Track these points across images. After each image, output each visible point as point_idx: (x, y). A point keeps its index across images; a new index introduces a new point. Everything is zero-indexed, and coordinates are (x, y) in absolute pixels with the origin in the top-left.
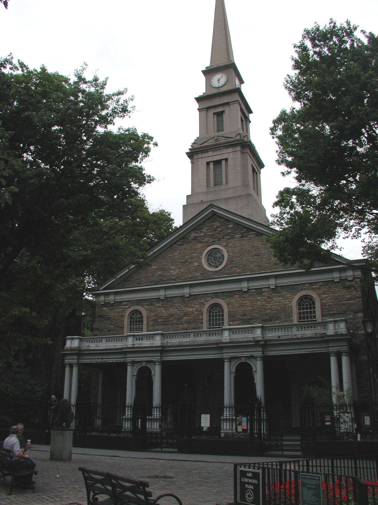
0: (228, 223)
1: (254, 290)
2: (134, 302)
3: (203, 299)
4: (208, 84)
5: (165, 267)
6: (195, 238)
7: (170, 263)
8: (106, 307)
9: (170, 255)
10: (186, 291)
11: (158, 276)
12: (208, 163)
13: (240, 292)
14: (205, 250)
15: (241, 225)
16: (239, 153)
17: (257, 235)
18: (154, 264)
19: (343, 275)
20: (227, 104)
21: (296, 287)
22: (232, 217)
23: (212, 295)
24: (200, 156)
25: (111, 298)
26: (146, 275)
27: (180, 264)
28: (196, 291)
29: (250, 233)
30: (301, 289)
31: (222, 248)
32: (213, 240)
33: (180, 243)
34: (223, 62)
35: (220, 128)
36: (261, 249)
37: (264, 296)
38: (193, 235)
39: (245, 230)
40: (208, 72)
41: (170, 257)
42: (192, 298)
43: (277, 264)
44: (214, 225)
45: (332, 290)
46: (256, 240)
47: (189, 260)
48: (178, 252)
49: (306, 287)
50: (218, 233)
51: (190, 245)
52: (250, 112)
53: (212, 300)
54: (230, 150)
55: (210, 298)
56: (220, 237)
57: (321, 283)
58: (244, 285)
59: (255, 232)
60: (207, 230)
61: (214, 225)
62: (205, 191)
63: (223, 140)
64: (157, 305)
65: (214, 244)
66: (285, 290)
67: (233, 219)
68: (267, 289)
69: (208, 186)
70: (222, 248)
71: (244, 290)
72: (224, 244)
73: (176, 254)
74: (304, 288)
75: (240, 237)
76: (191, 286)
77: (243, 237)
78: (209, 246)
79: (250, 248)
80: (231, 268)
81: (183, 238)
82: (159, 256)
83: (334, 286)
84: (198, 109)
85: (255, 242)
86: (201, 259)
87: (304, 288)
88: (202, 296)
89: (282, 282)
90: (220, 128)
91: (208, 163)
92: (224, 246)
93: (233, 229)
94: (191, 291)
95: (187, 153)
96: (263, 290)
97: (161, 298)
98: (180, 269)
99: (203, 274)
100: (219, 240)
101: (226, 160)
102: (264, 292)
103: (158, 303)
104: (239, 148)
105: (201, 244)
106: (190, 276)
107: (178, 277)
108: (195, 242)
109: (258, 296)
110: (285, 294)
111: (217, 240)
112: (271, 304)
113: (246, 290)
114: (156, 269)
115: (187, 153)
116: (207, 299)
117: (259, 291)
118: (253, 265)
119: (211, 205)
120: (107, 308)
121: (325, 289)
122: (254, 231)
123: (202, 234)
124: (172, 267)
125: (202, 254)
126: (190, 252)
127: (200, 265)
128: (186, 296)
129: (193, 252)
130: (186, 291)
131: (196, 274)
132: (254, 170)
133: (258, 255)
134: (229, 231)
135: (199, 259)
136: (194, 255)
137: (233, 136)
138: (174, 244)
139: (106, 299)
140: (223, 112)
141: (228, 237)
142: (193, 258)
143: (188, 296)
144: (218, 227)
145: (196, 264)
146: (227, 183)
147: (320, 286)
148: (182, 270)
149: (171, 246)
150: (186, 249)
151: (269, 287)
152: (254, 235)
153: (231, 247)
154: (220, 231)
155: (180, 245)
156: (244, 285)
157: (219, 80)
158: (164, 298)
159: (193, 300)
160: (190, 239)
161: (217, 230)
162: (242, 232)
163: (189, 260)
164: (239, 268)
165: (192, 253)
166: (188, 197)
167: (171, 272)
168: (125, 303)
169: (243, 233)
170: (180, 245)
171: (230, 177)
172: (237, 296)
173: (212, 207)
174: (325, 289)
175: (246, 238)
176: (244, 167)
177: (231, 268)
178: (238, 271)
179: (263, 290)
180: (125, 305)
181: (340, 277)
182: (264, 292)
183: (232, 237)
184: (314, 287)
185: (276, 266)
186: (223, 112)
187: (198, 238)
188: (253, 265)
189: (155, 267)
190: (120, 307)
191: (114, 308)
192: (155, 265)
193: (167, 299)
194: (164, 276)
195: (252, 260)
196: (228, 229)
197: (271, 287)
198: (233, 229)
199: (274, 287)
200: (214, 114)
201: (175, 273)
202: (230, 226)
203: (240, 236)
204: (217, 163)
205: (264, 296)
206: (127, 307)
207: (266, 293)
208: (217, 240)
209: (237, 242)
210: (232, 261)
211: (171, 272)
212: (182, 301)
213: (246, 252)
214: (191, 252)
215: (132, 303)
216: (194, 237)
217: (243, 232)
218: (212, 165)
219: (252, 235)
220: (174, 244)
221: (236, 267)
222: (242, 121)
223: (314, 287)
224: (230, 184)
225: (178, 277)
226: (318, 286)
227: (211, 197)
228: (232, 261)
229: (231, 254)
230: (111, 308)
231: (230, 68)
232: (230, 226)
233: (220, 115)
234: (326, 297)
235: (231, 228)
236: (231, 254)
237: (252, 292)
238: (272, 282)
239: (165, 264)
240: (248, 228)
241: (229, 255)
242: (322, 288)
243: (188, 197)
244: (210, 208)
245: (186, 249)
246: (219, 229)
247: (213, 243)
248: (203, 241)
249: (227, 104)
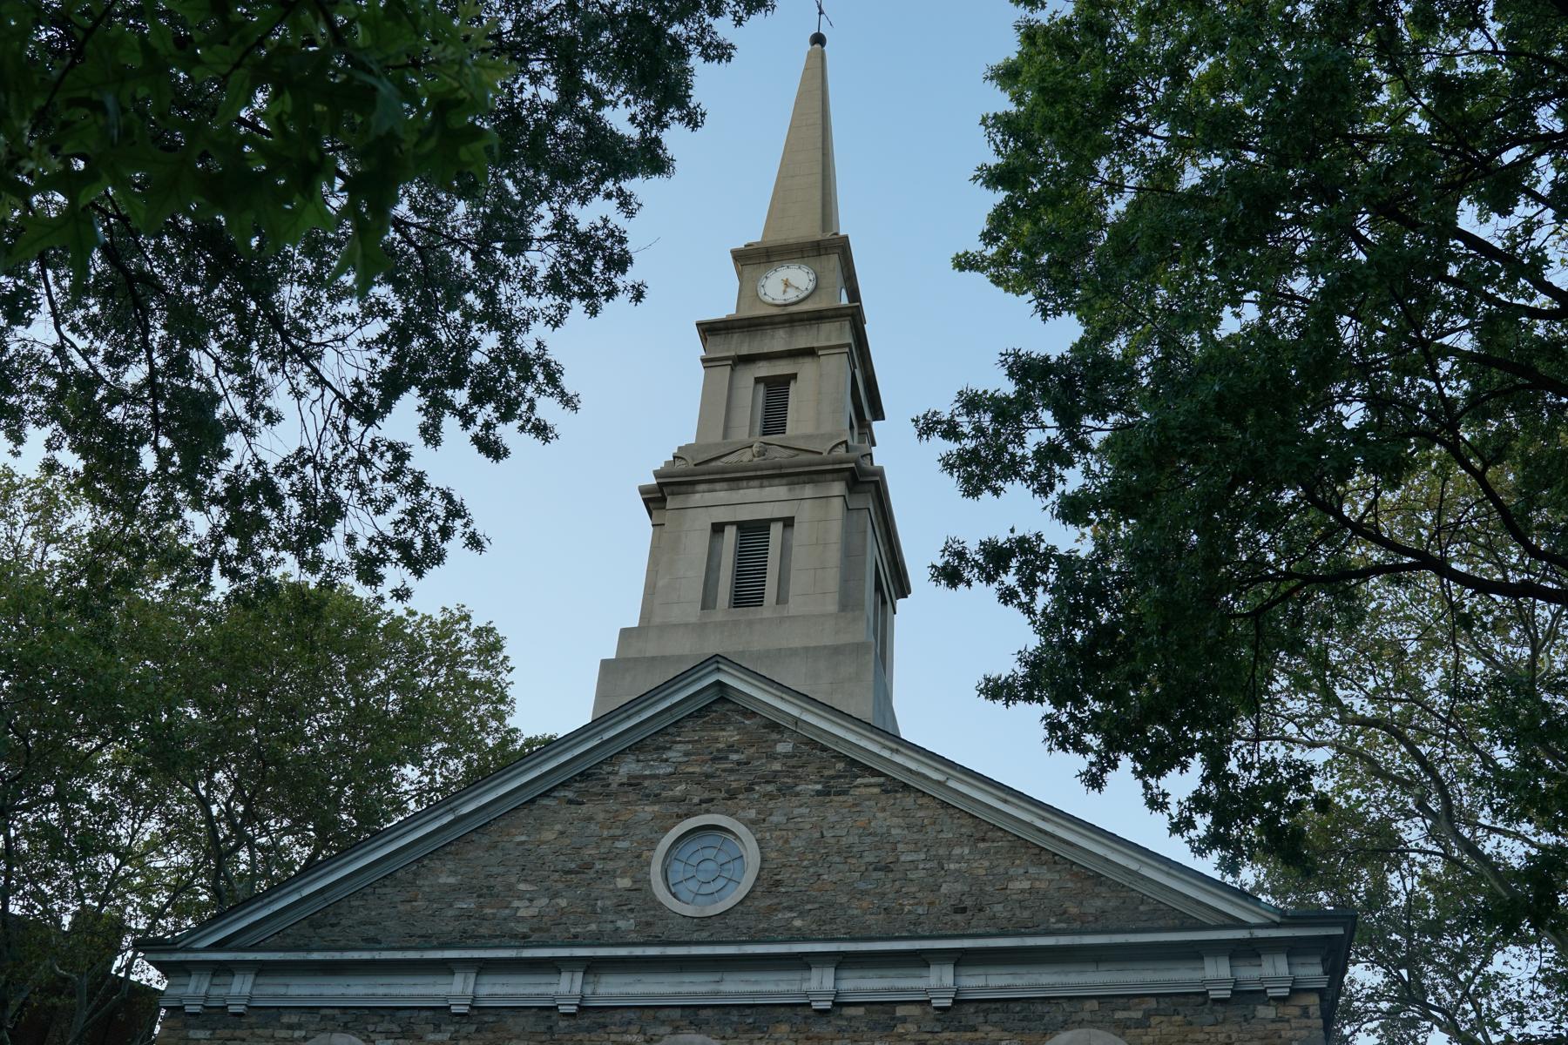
0: (775, 736)
1: (861, 1011)
2: (333, 1018)
3: (634, 1029)
4: (748, 291)
5: (492, 881)
6: (634, 783)
7: (514, 870)
8: (204, 1027)
9: (523, 838)
10: (567, 987)
11: (457, 918)
12: (718, 528)
13: (799, 1010)
14: (667, 830)
15: (824, 749)
16: (837, 504)
17: (886, 792)
18: (450, 865)
19: (1249, 973)
20: (810, 352)
21: (1039, 1008)
22: (795, 712)
23: (679, 1012)
24: (697, 499)
25: (241, 986)
26: (408, 907)
27: (556, 876)
28: (613, 989)
29: (859, 781)
30: (1065, 1022)
31: (740, 829)
32: (706, 795)
33: (570, 795)
34: (807, 230)
35: (774, 420)
36: (900, 846)
38: (628, 768)
39: (840, 766)
40: (751, 259)
41: (523, 843)
42: (586, 1022)
43: (964, 910)
44: (716, 740)
45: (1200, 1037)
46: (884, 810)
47: (599, 866)
48: (558, 827)
49: (1087, 1016)
50: (731, 771)
51: (612, 804)
52: (879, 414)
53: (673, 1038)
54: (808, 491)
55: (668, 1029)
56: (734, 785)
57: (1153, 1004)
58: (820, 983)
59: (882, 780)
60: (686, 754)
61: (716, 740)
62: (694, 620)
63: (779, 456)
64: (431, 1037)
65: (708, 811)
66: (994, 1017)
67: (797, 721)
68: (915, 1011)
69: (708, 602)
70: (740, 829)
71: (815, 1006)
72: (752, 814)
73: (549, 835)
74: (1075, 1018)
75: (818, 793)
76: (593, 967)
77: (828, 794)
78: (688, 816)
79: (851, 840)
80: (773, 909)
81: (584, 776)
82: (475, 837)
83: (1211, 1019)
84: (704, 360)
85: (879, 815)
86: (649, 864)
87: (1075, 1018)
88: (631, 1015)
89: (978, 982)
90: (774, 420)
91: (718, 528)
92: (751, 824)
93: (794, 762)
94: (588, 990)
95: (644, 491)
96: (900, 1011)
97: (454, 1009)
98: (556, 895)
99: (648, 924)
100: (732, 795)
101: (788, 522)
102: (904, 1020)
103: (437, 1028)
104: (838, 488)
105: (656, 808)
106: (593, 927)
107: (540, 929)
108: (632, 797)
109: (876, 1034)
111: (723, 795)
113: (828, 1005)
114: (454, 889)
115: (644, 491)
116: (651, 1031)
117: (883, 1012)
118: (865, 905)
119: (716, 659)
120: (206, 1034)
121: (1165, 1028)
122: (880, 774)
123: (664, 770)
124: (522, 887)
125: (652, 844)
126: (605, 833)
127: (641, 887)
128: (562, 1009)
129: (618, 832)
130: (567, 987)
131: (620, 923)
132: (878, 587)
133: (887, 869)
134: (777, 766)
135: (640, 863)
136: (619, 844)
137: (824, 447)
138: (545, 795)
139: (215, 991)
140: (794, 376)
141: (770, 788)
142: (617, 857)
143: (573, 1009)
144: (731, 748)
145: (624, 883)
146: (781, 599)
147: (1148, 1015)
148: (563, 903)
149: (532, 801)
150: (590, 819)
151: (929, 1002)
152: (876, 790)
153: (777, 827)
154: (739, 763)
155: (570, 802)
156: (820, 983)
157: (787, 284)
158: (465, 1010)
159: (588, 1030)
160: (614, 781)
161: (727, 758)
162: (826, 773)
163: (599, 866)
164: (801, 915)
165: (615, 838)
166: (625, 633)
167: (516, 904)
168: (294, 1019)
169: (833, 777)
170: (570, 802)
171: (799, 582)
172: (785, 1028)
173: (718, 669)
174: (1165, 1028)
175: (841, 798)
176: (850, 555)
177: (773, 909)
178: (798, 923)
179: (900, 1011)
180: (291, 1027)
181: (1236, 983)
182: (904, 1020)
183: (784, 791)
184: (1119, 1015)
185: (958, 917)
186: (794, 376)
187: (646, 783)
188: (865, 905)
189: (452, 880)
190: (268, 1032)
191: (238, 1033)
192: (453, 873)
193: (478, 1014)
194: (484, 918)
195: (862, 886)
196: (772, 757)
197: (935, 1003)
198: (794, 762)
199: (948, 1003)
200: (758, 380)
201: (533, 911)
202: (781, 748)
203: (819, 787)
204: (753, 531)
206: (297, 1034)
207: (912, 1028)
208: (723, 795)
209: (804, 810)
210: (778, 883)
211: (516, 904)
212: (542, 1028)
213: (839, 853)
214: (612, 832)
215: (323, 1018)
216: (636, 777)
217: (832, 772)
218: (731, 534)
219: (866, 787)
220: (545, 795)
221: (790, 909)
222: (851, 427)
223: (1119, 1015)
224: (795, 606)
225: (540, 929)
226: (1139, 1015)
227: (713, 645)
228: (778, 883)
229: (773, 855)
230: (227, 1033)
231: (831, 251)
232: (781, 748)
233: (777, 388)
235: (786, 756)
236: (773, 855)
237: (850, 1019)
238: (940, 980)
239: (495, 870)
240: (853, 762)
241: (763, 860)
242: (1154, 1020)
243: (625, 633)
244: (710, 673)
245: (590, 819)
246: (734, 757)
247: (707, 804)
248: (664, 794)
249: (810, 352)
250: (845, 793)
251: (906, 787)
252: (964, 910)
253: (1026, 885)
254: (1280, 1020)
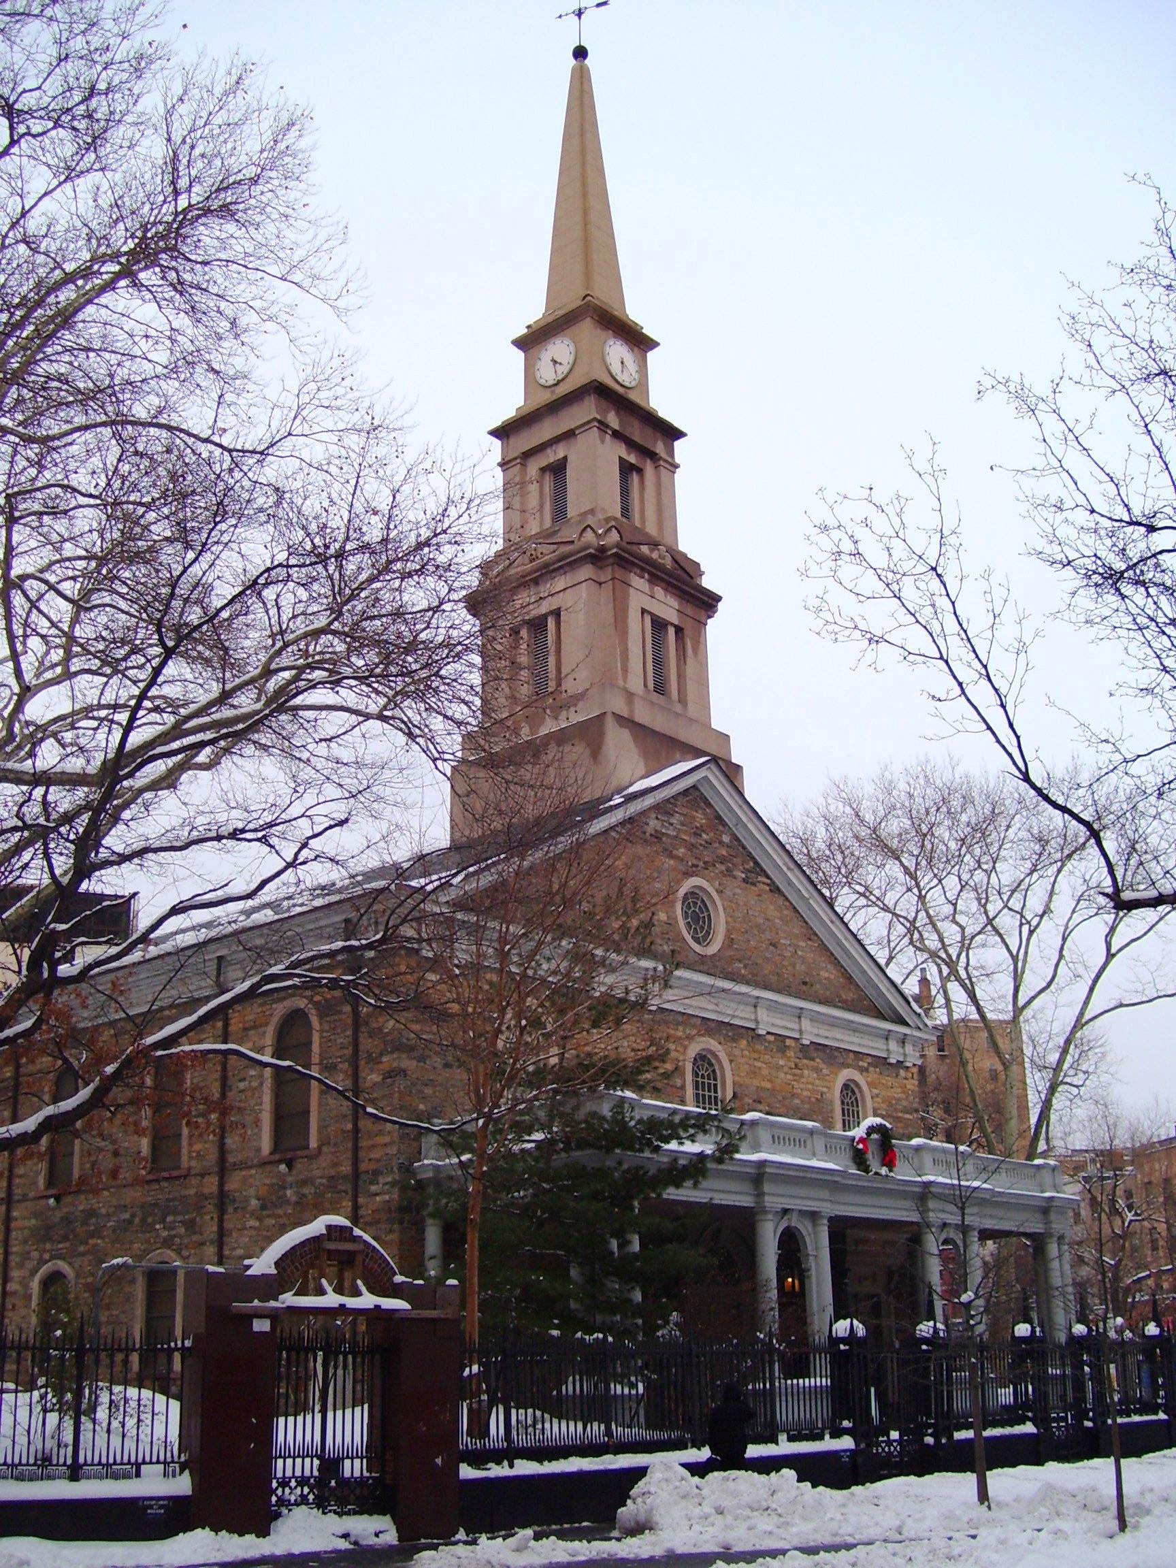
0: (721, 828)
1: (771, 1038)
29: (760, 879)
37: (789, 1058)
43: (805, 983)
57: (869, 1060)
66: (821, 1054)
102: (788, 1047)
110: (822, 1065)
112: (802, 1086)
141: (723, 868)
179: (788, 1042)
184: (861, 1063)
185: (804, 988)
205: (789, 1058)
221: (740, 961)
223: (861, 1063)
226: (865, 1065)
234: (877, 1096)
242: (871, 1069)
246: (704, 836)
250: (754, 884)
251: (778, 890)
252: (805, 983)
253: (826, 975)
254: (906, 1078)
